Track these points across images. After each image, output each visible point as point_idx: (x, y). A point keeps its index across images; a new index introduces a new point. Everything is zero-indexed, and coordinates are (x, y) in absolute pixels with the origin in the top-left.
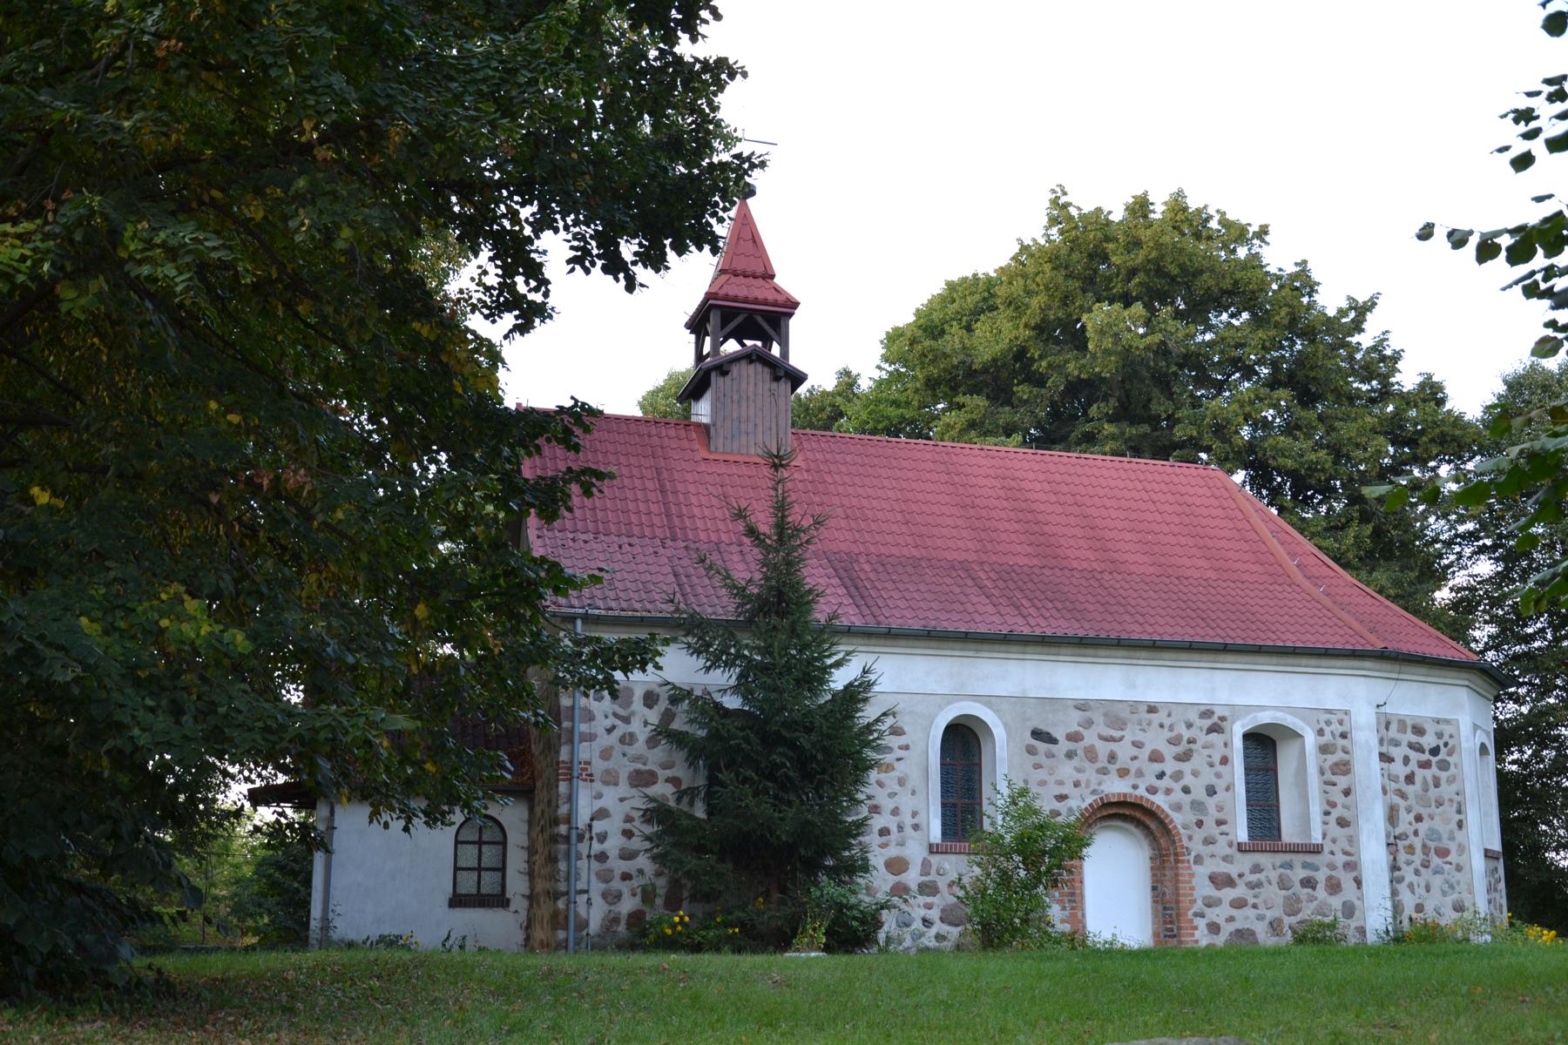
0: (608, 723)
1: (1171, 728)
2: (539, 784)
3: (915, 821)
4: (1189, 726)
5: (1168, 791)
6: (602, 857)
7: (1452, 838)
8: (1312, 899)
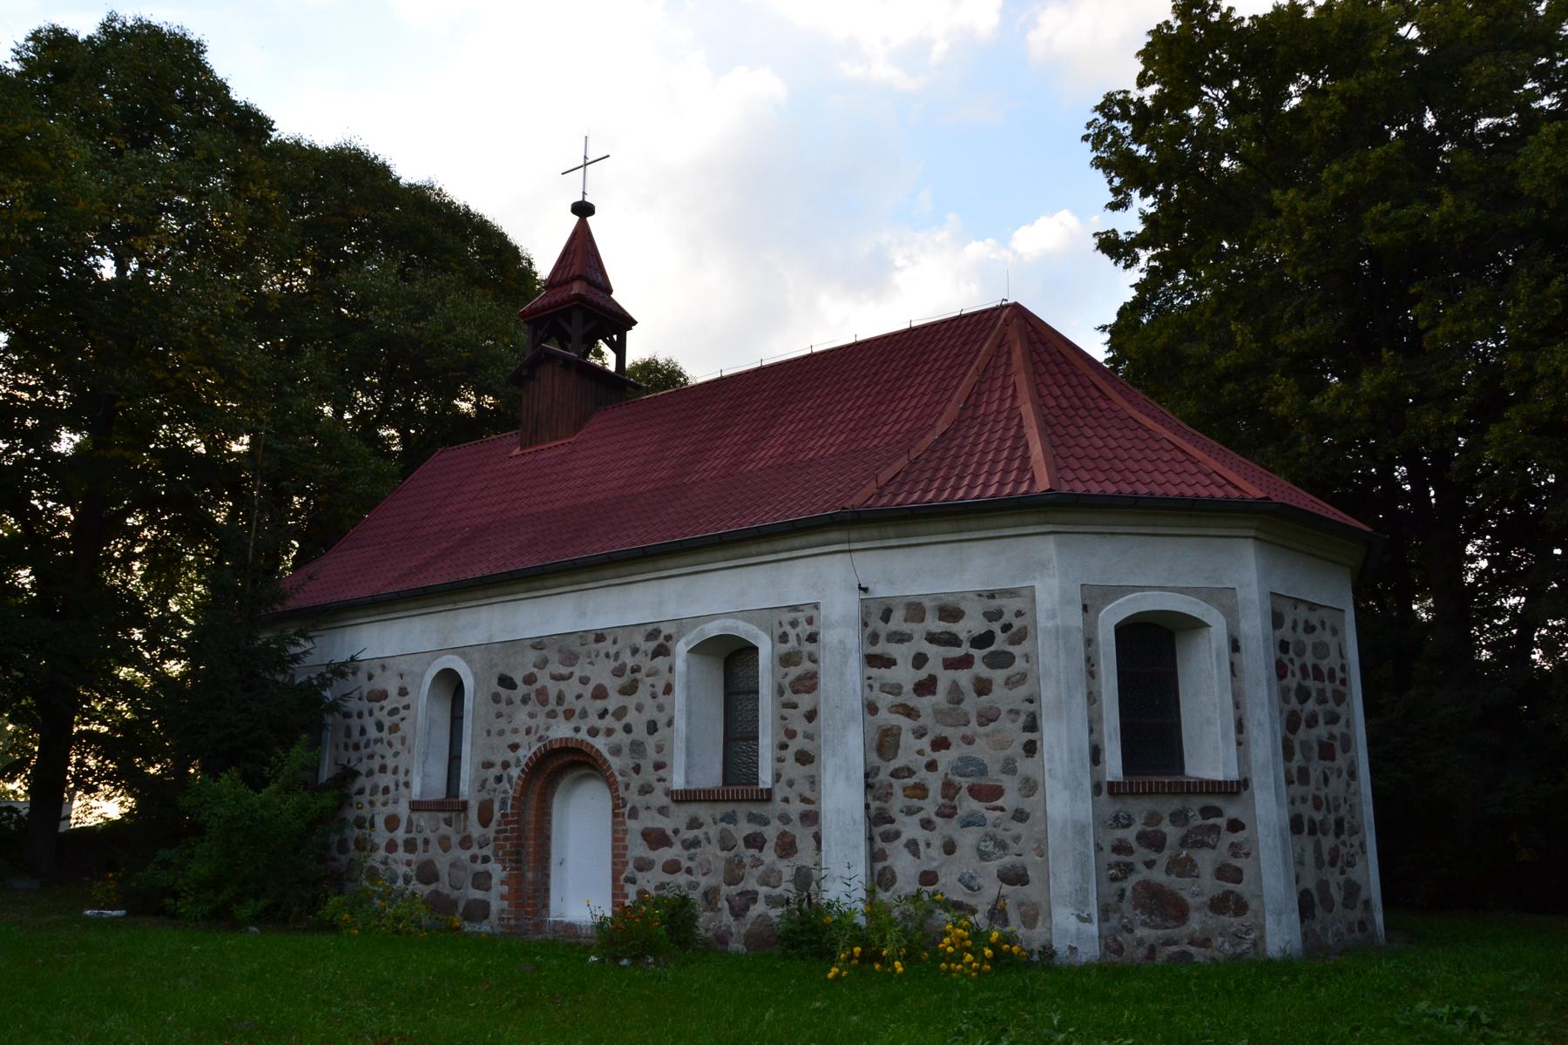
1: (617, 655)
4: (635, 651)
5: (609, 732)
7: (1009, 768)
8: (757, 863)
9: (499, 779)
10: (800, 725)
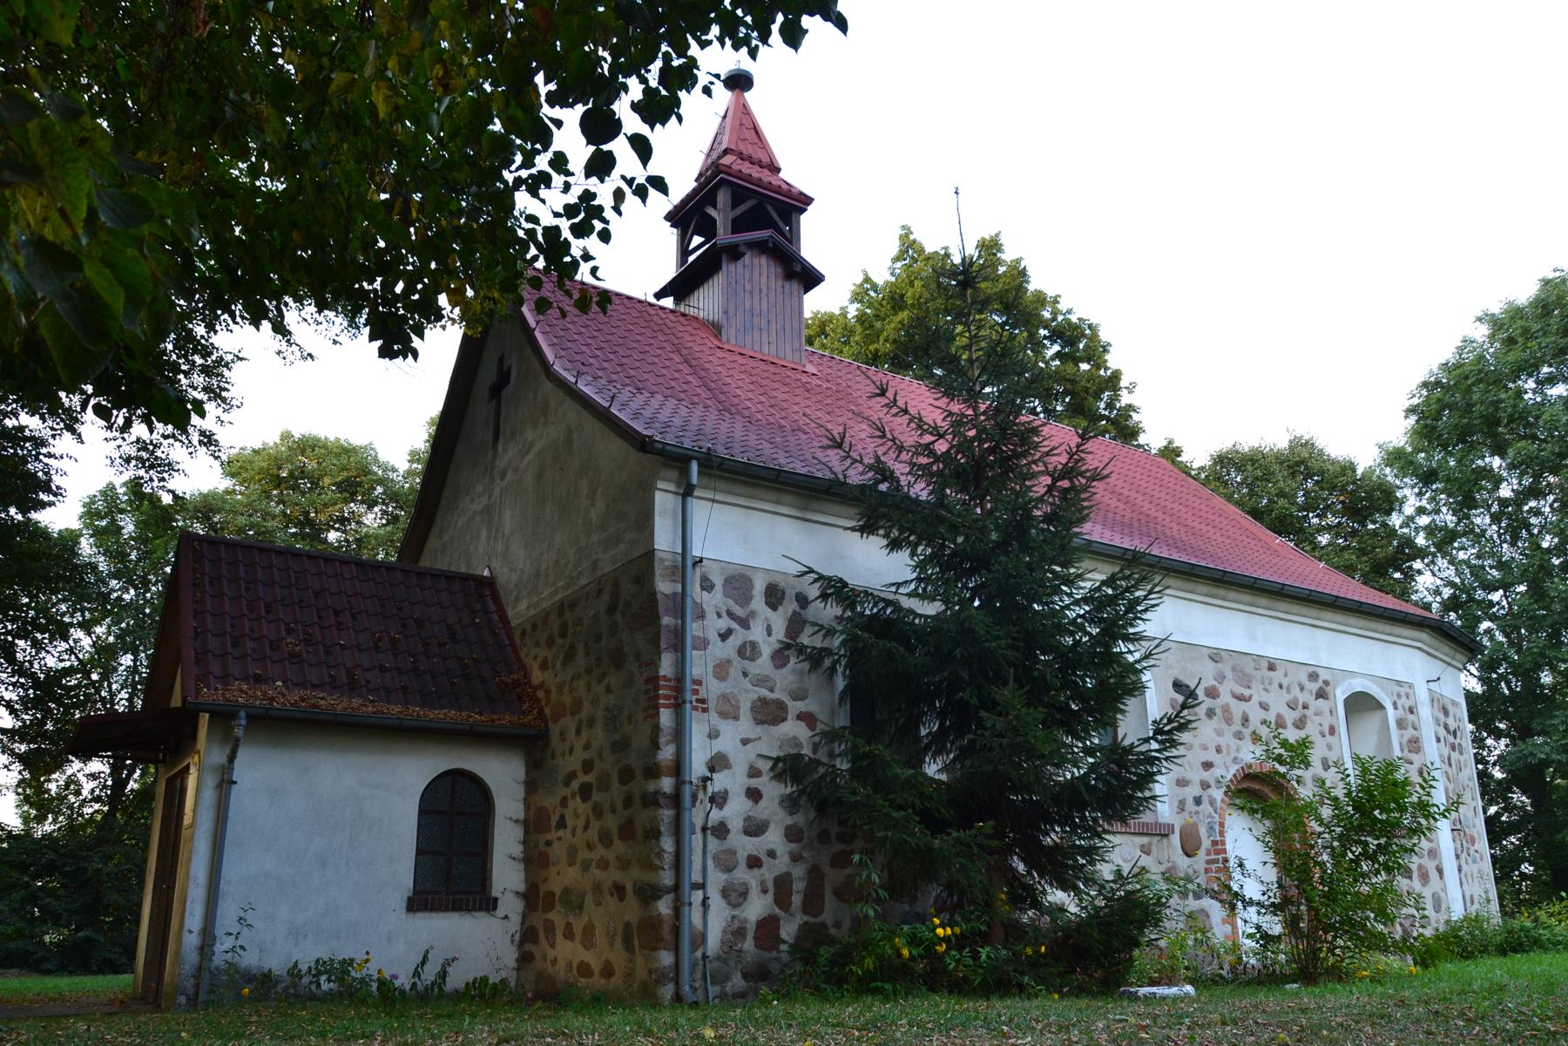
0: (725, 623)
6: (721, 830)
9: (1198, 801)
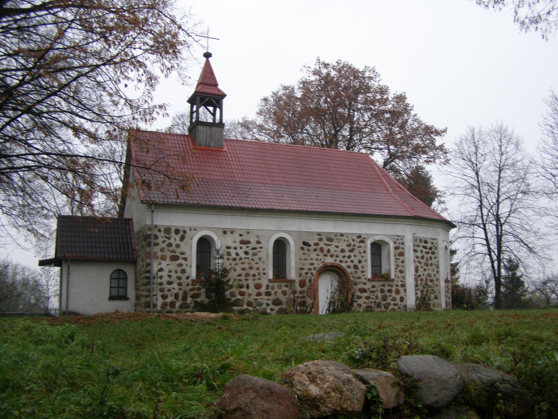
0: (163, 240)
1: (348, 241)
2: (139, 259)
3: (264, 272)
4: (353, 240)
5: (346, 262)
6: (161, 284)
7: (435, 276)
8: (391, 296)
9: (307, 273)
10: (400, 264)
